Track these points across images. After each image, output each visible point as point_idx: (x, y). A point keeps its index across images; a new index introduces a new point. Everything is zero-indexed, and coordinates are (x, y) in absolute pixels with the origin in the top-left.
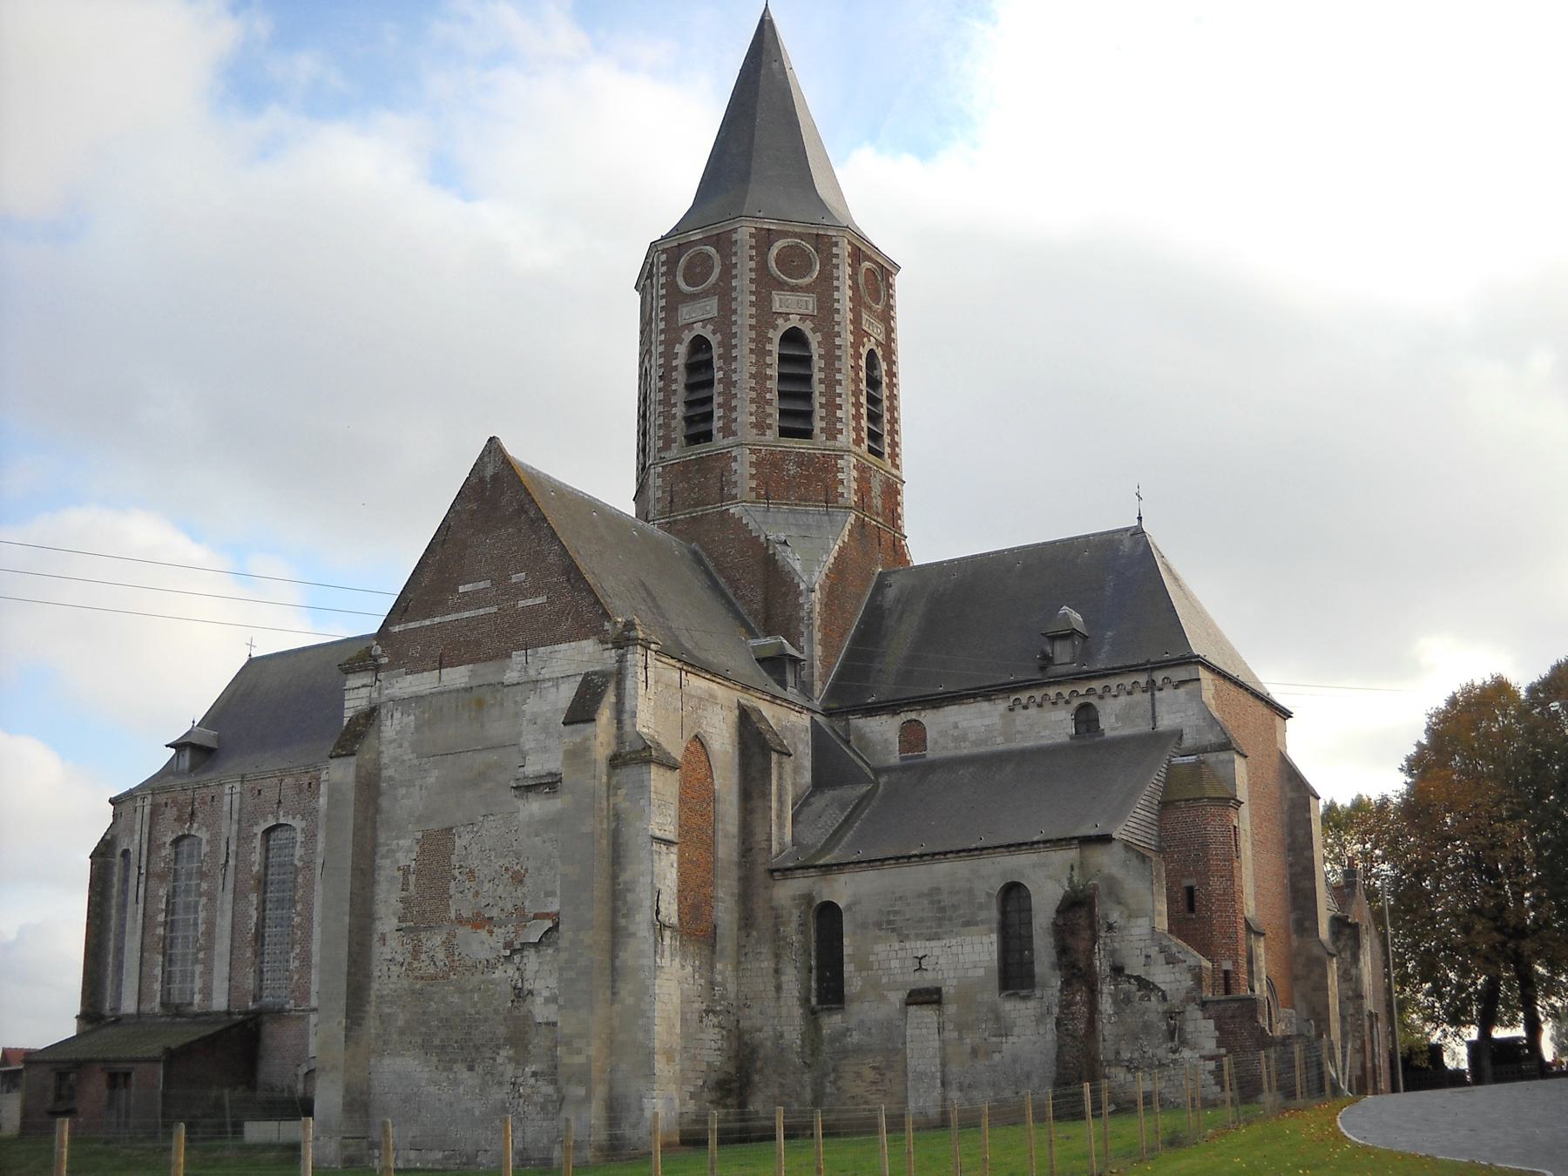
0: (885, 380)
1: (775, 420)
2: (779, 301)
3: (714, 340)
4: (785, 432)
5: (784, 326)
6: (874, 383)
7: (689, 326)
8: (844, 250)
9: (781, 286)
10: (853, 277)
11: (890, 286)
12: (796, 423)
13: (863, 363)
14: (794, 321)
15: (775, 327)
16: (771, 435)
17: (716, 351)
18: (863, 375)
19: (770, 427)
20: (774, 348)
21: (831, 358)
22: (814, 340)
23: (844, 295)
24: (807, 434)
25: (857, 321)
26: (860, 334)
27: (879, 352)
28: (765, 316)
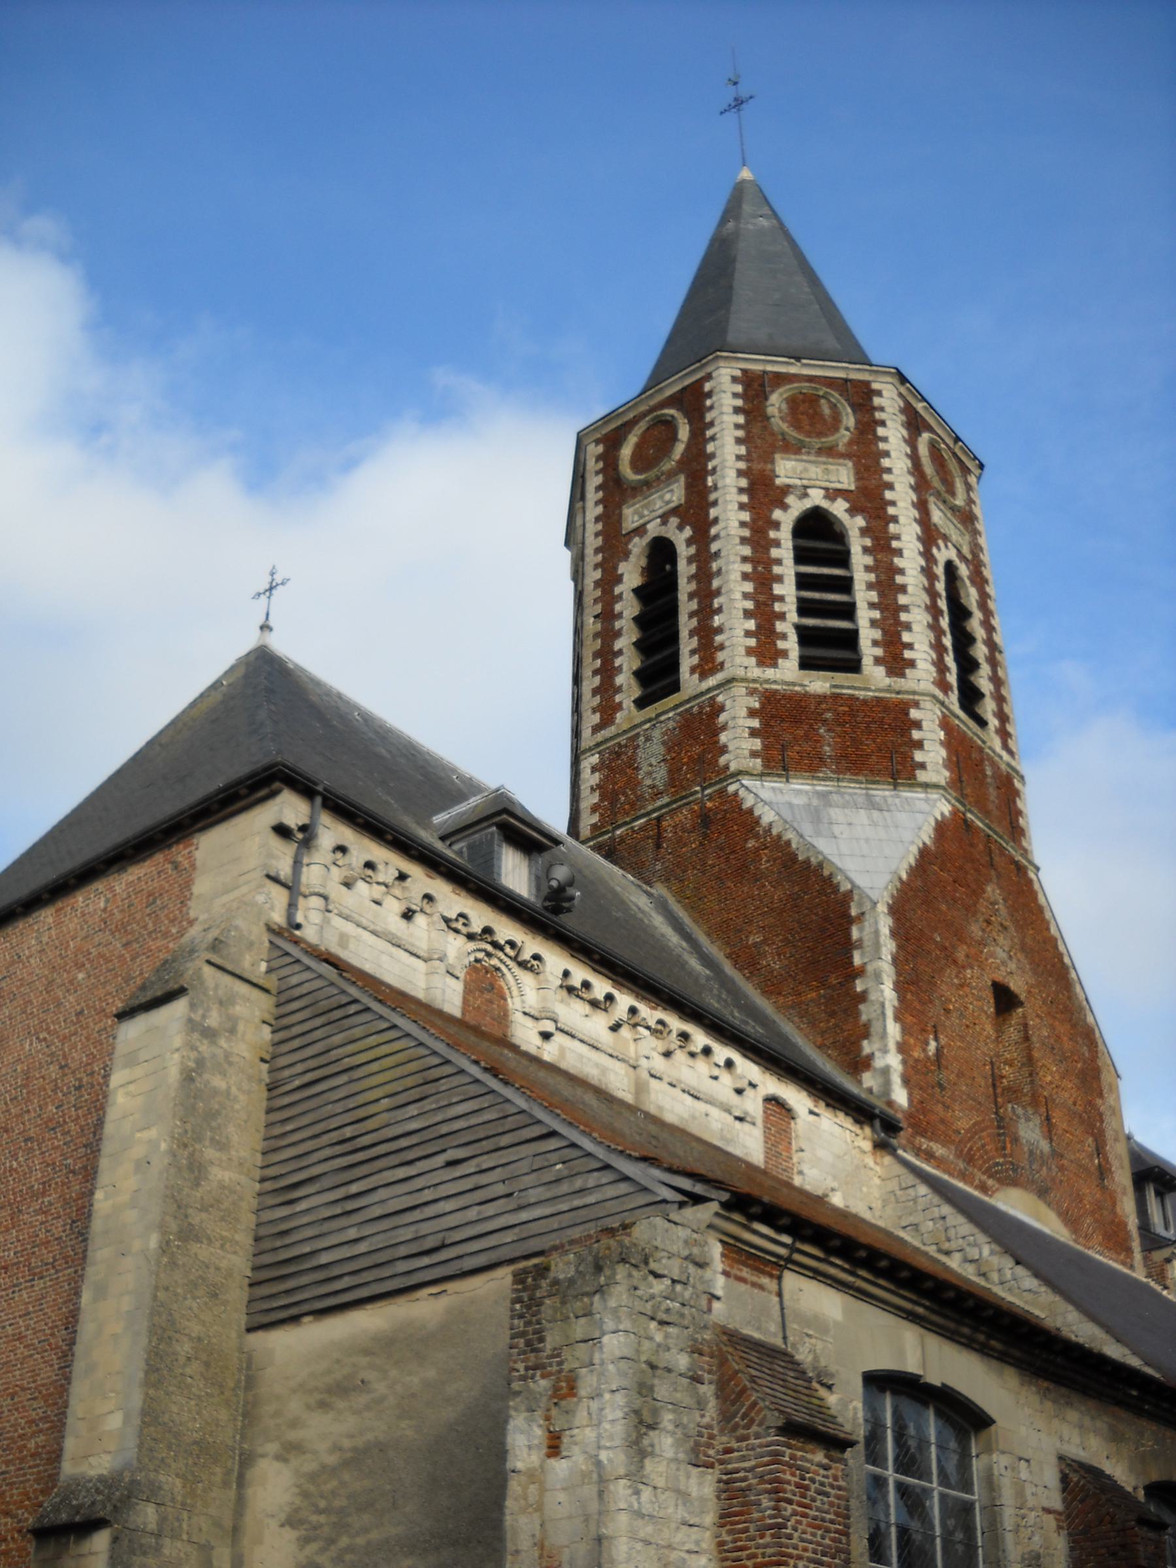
1: (791, 645)
2: (786, 469)
3: (681, 538)
4: (806, 664)
5: (797, 507)
6: (959, 613)
7: (640, 531)
8: (888, 399)
9: (792, 448)
14: (816, 498)
15: (785, 507)
17: (684, 551)
19: (784, 654)
22: (854, 525)
23: (897, 464)
25: (924, 520)
26: (930, 536)
27: (963, 571)
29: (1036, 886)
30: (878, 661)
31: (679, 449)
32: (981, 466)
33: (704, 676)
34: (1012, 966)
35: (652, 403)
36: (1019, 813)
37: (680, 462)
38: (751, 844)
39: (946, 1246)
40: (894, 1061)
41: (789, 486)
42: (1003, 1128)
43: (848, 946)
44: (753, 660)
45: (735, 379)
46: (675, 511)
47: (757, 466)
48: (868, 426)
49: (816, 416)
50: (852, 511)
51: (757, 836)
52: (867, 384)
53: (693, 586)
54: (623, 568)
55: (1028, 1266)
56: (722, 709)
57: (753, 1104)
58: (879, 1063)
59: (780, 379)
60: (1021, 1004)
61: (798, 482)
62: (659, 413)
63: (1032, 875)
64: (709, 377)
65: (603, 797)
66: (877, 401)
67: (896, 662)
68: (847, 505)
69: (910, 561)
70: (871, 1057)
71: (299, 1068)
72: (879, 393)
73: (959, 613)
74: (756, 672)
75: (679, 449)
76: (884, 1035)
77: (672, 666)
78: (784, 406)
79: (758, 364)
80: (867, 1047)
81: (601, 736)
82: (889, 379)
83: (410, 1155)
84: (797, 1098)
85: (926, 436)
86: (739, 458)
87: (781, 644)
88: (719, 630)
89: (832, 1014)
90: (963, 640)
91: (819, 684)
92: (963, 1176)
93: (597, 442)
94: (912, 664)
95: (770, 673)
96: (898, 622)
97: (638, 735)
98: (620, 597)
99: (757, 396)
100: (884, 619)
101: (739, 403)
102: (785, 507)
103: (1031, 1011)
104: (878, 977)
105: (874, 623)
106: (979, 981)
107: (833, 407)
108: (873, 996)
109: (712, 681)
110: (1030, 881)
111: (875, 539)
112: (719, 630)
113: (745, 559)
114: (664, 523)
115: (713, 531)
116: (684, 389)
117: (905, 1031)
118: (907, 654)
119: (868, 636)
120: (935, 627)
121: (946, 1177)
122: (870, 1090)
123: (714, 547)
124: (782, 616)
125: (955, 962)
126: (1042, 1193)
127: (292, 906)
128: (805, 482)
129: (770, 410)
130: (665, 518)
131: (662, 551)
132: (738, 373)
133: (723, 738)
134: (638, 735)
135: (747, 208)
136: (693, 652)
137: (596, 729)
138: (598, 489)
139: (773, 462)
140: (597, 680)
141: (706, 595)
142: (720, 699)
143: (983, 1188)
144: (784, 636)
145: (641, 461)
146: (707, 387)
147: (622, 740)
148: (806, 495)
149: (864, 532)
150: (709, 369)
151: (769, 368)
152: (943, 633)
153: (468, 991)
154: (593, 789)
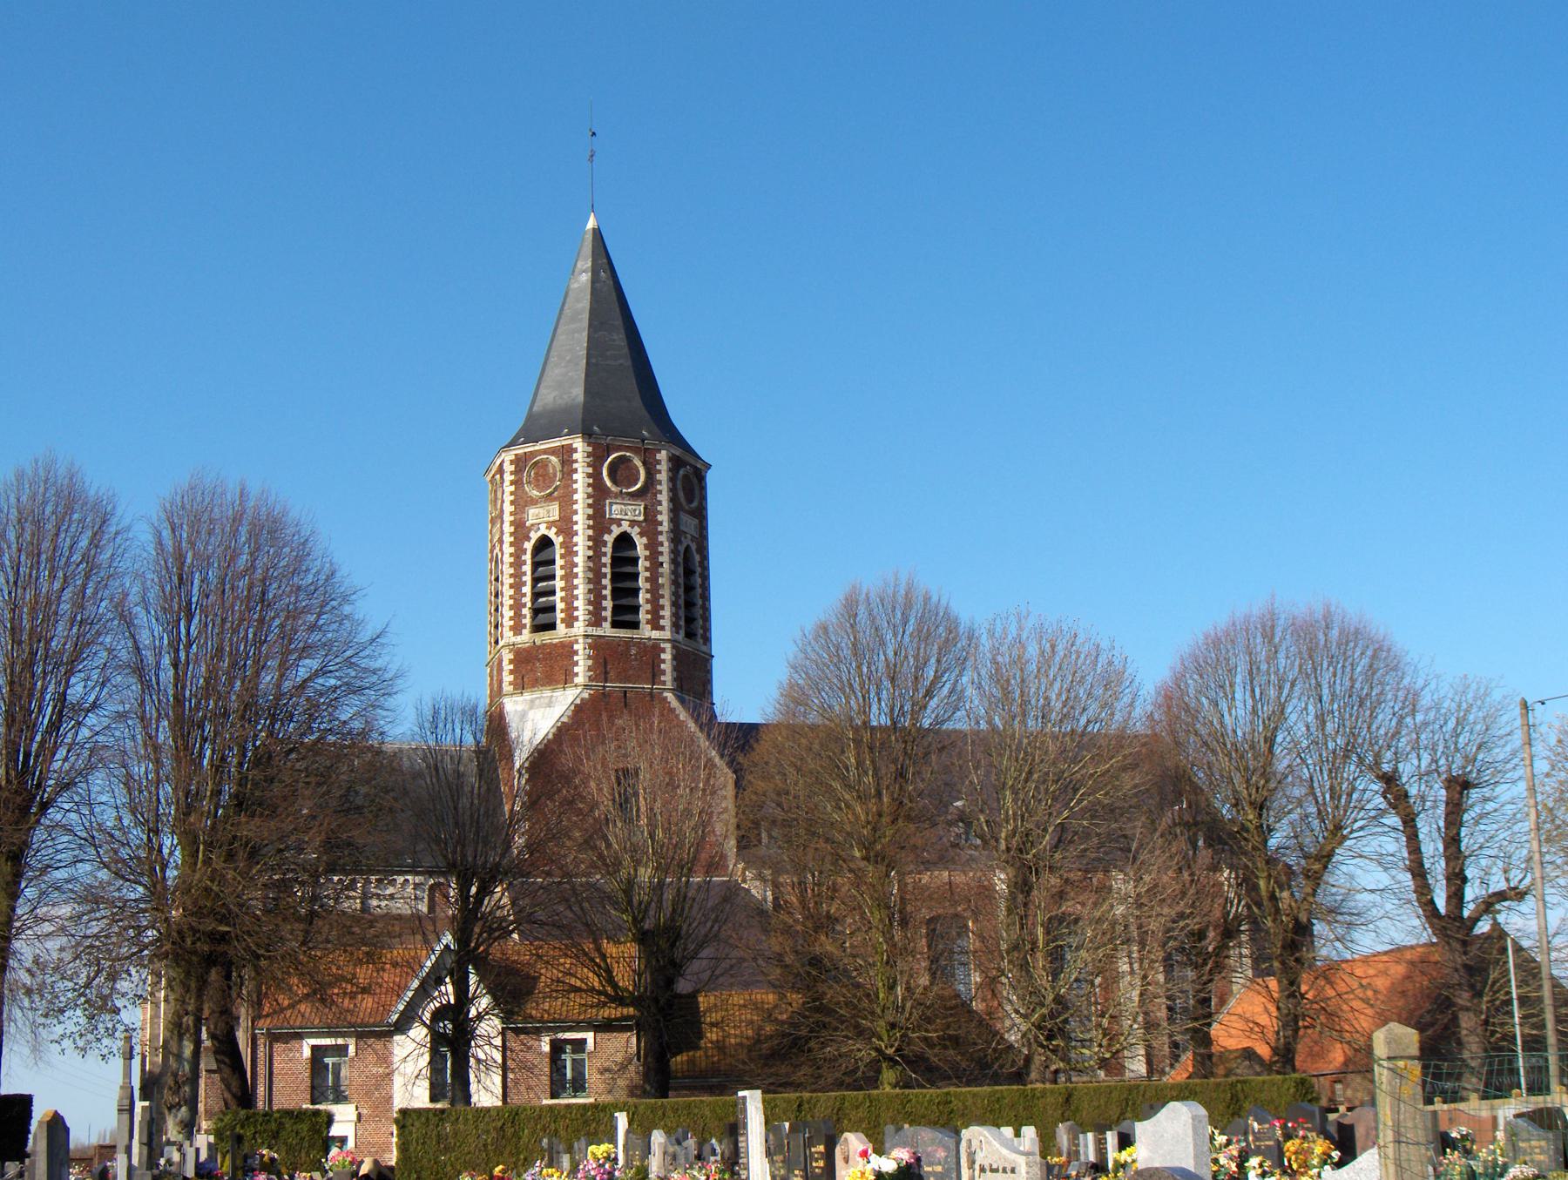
0: (699, 570)
2: (615, 510)
3: (558, 541)
6: (689, 572)
7: (536, 526)
12: (625, 616)
17: (559, 551)
22: (640, 542)
24: (635, 625)
27: (694, 547)
28: (599, 523)
50: (641, 534)
102: (610, 532)
131: (545, 543)
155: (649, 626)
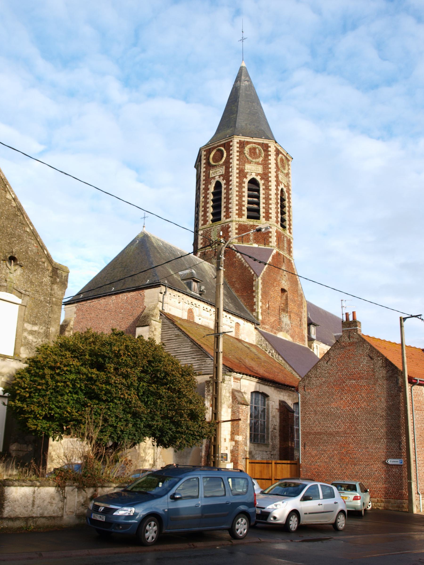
1: (245, 213)
2: (248, 168)
3: (223, 182)
4: (249, 217)
5: (249, 178)
6: (282, 200)
7: (214, 178)
8: (272, 150)
9: (250, 162)
10: (276, 160)
11: (289, 165)
13: (279, 192)
14: (254, 176)
15: (246, 178)
16: (245, 218)
17: (224, 186)
18: (279, 197)
19: (244, 215)
20: (246, 185)
21: (267, 188)
22: (261, 182)
26: (278, 183)
27: (285, 190)
28: (242, 174)
29: (293, 264)
30: (264, 217)
31: (224, 159)
32: (292, 159)
33: (227, 218)
34: (286, 284)
35: (218, 144)
36: (291, 247)
37: (224, 162)
38: (234, 259)
39: (266, 349)
40: (260, 311)
41: (248, 172)
42: (280, 321)
43: (252, 286)
44: (237, 216)
45: (237, 143)
46: (221, 175)
47: (241, 167)
48: (267, 156)
49: (255, 153)
50: (261, 179)
51: (236, 258)
52: (267, 144)
53: (225, 196)
54: (209, 186)
55: (281, 356)
56: (230, 227)
57: (233, 325)
58: (257, 311)
59: (248, 143)
60: (287, 292)
61: (249, 171)
62: (220, 148)
63: (292, 262)
64: (231, 141)
65: (203, 242)
66: (269, 149)
67: (267, 218)
68: (260, 177)
69: (273, 192)
70: (255, 309)
71: (166, 337)
72: (270, 147)
73: (282, 200)
74: (238, 219)
75: (224, 159)
76: (258, 306)
77: (220, 213)
78: (248, 150)
79: (243, 139)
80: (255, 307)
81: (204, 227)
82: (273, 143)
83: (187, 355)
84: (240, 321)
85: (280, 155)
86: (237, 165)
87: (243, 213)
88: (230, 208)
89: (248, 299)
90: (283, 206)
91: (251, 222)
92: (271, 331)
93: (205, 151)
94: (271, 218)
95: (241, 219)
96: (269, 208)
97: (211, 229)
98: (208, 194)
99: (242, 147)
100: (266, 206)
101: (238, 149)
102: (246, 178)
103: (289, 294)
104: (258, 293)
105: (264, 208)
106: (278, 289)
107: (260, 150)
108: (256, 297)
109: (228, 220)
110: (291, 263)
111: (266, 186)
112: (230, 208)
113: (237, 191)
114: (219, 177)
115: (230, 183)
116: (225, 143)
117: (262, 303)
118: (270, 215)
119: (262, 210)
120: (277, 208)
121: (268, 332)
122: (254, 316)
123: (230, 187)
124: (244, 206)
125: (274, 286)
126: (287, 332)
127: (163, 306)
128: (252, 171)
129: (246, 152)
130: (220, 176)
132: (238, 141)
133: (230, 234)
134: (211, 229)
135: (243, 78)
136: (224, 212)
137: (202, 225)
138: (204, 164)
139: (245, 166)
140: (203, 213)
141: (228, 199)
142: (230, 224)
143: (275, 333)
144: (244, 211)
145: (215, 160)
146: (231, 144)
147: (208, 229)
148: (251, 175)
149: (263, 184)
150: (232, 139)
151: (246, 140)
152: (278, 208)
153: (188, 314)
154: (201, 239)
155: (264, 219)
